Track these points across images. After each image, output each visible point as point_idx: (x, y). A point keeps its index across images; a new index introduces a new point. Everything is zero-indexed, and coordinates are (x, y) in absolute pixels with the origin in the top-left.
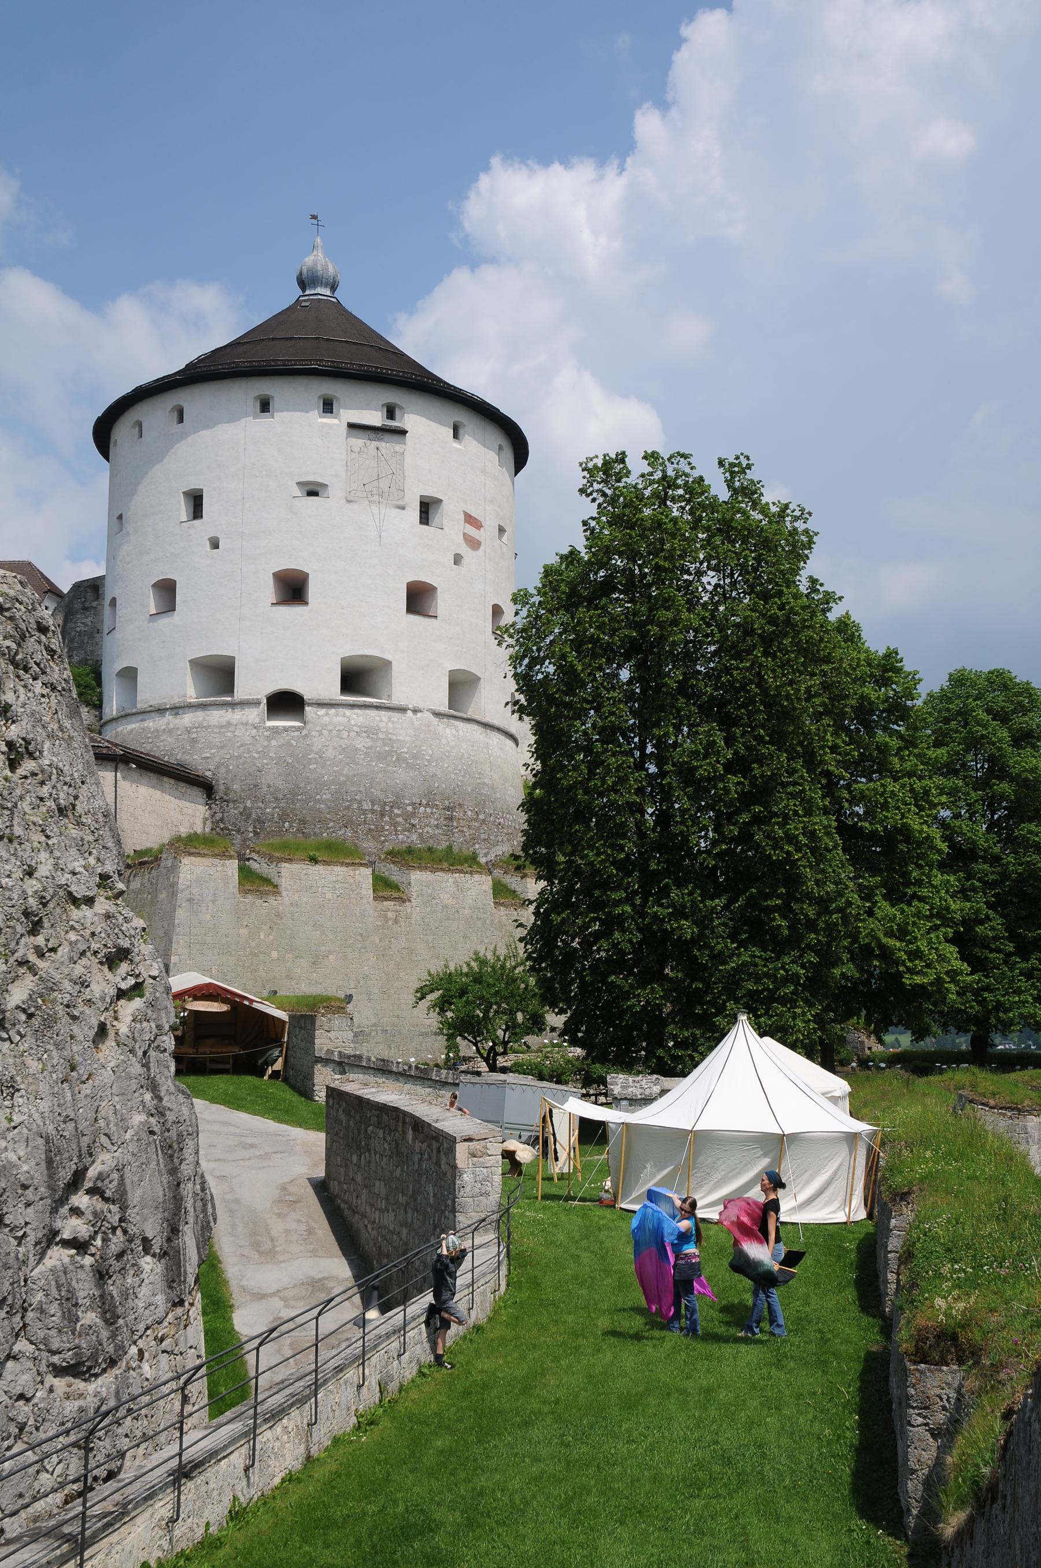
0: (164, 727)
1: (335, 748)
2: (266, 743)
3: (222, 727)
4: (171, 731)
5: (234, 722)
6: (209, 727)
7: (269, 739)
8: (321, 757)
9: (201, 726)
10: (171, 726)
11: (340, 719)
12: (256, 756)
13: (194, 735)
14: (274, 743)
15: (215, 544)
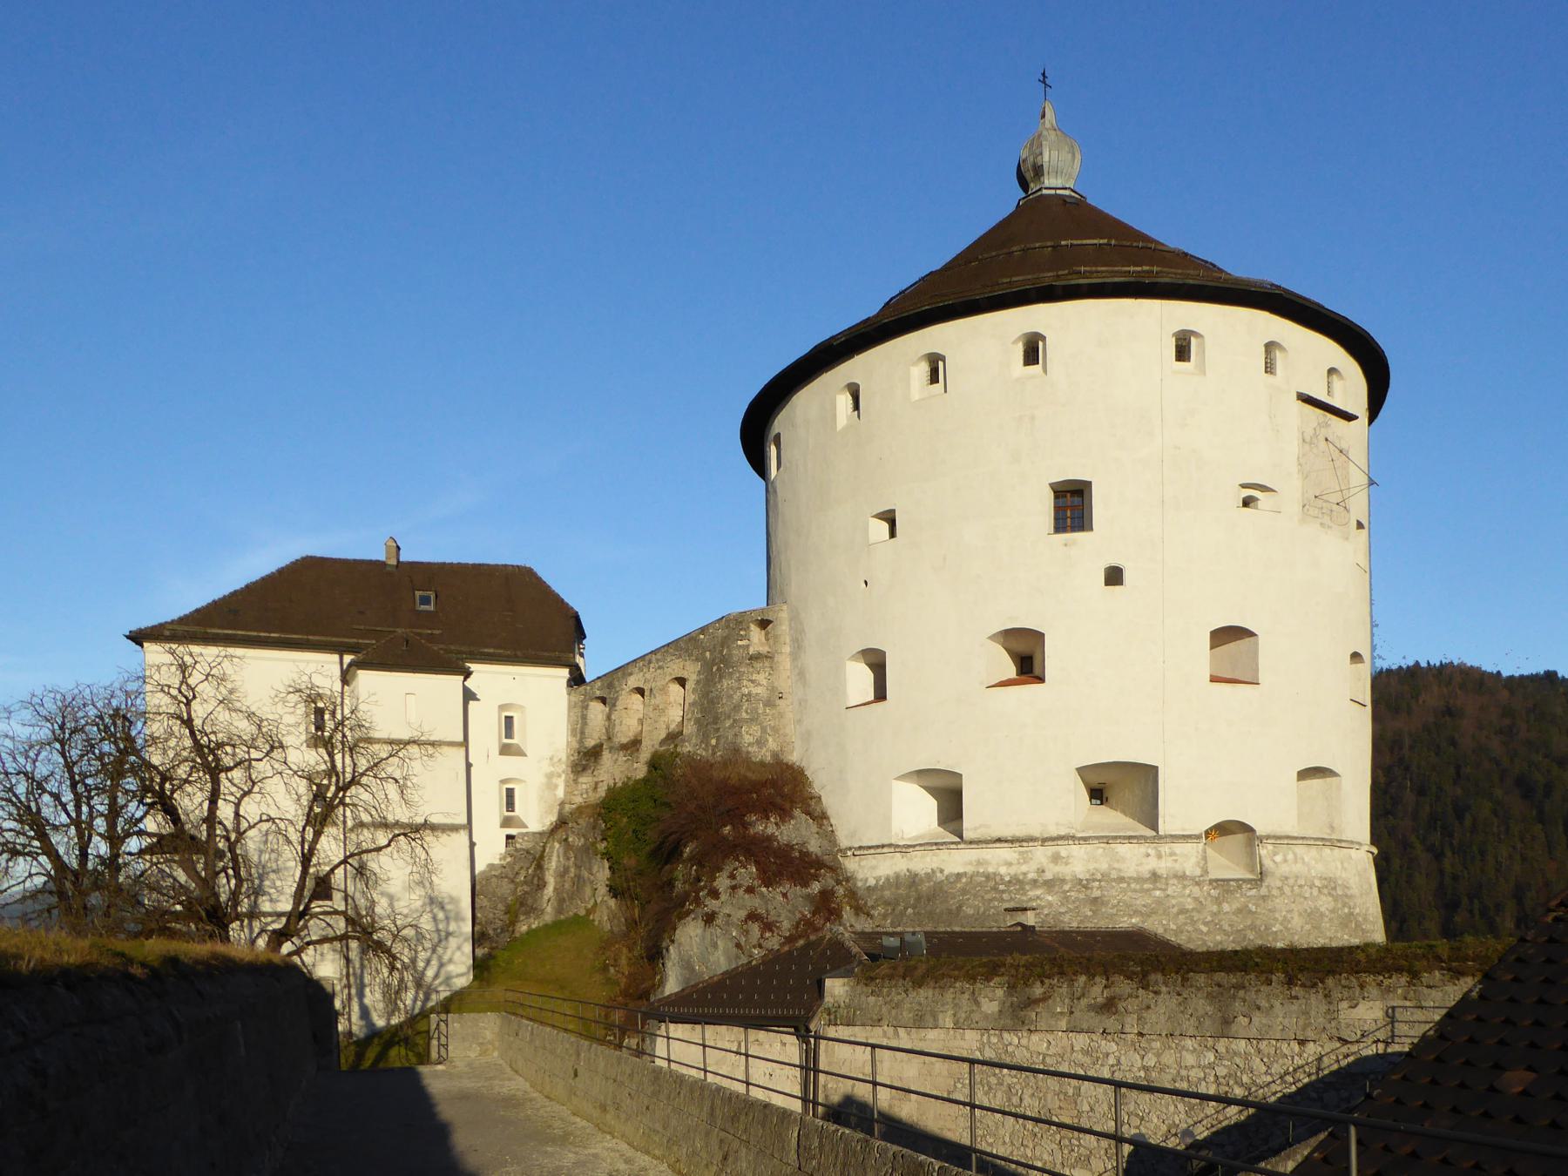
0: (1031, 876)
1: (1300, 914)
2: (1215, 908)
3: (1145, 880)
4: (1050, 884)
5: (1162, 872)
6: (1121, 879)
7: (1218, 901)
8: (1286, 928)
9: (1105, 877)
10: (1048, 876)
11: (1298, 868)
12: (1205, 929)
13: (1097, 893)
14: (1226, 907)
15: (1114, 576)
